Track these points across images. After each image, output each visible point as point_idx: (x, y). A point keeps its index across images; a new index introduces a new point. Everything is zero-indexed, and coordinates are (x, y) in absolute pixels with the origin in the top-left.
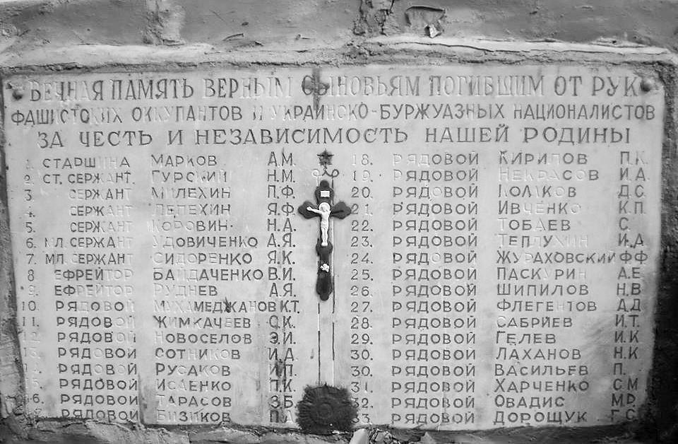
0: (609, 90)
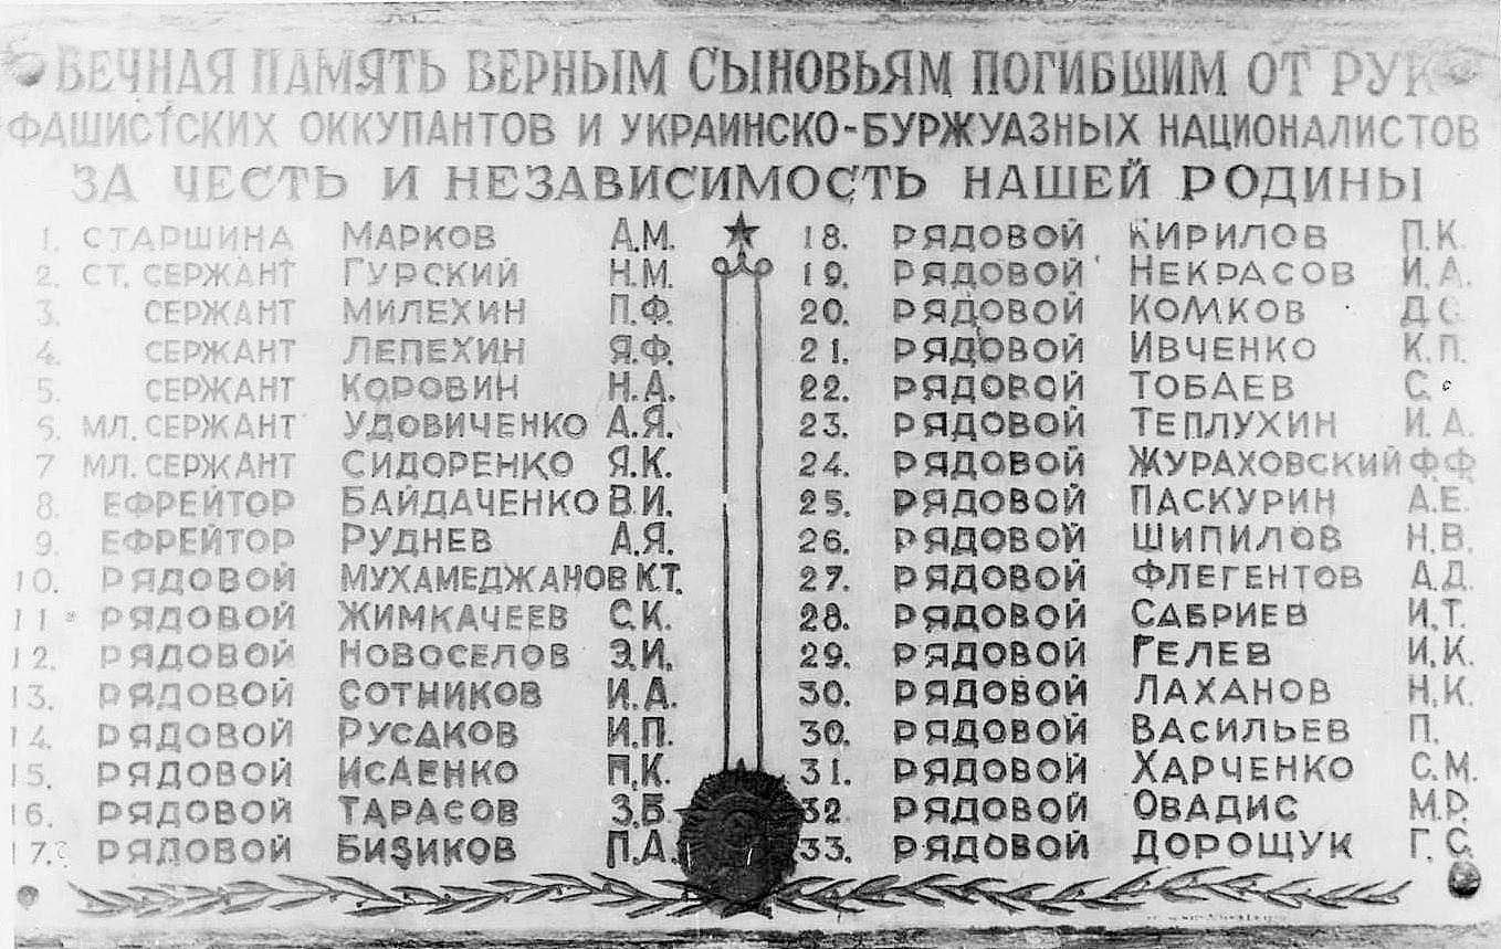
0: (1371, 82)
